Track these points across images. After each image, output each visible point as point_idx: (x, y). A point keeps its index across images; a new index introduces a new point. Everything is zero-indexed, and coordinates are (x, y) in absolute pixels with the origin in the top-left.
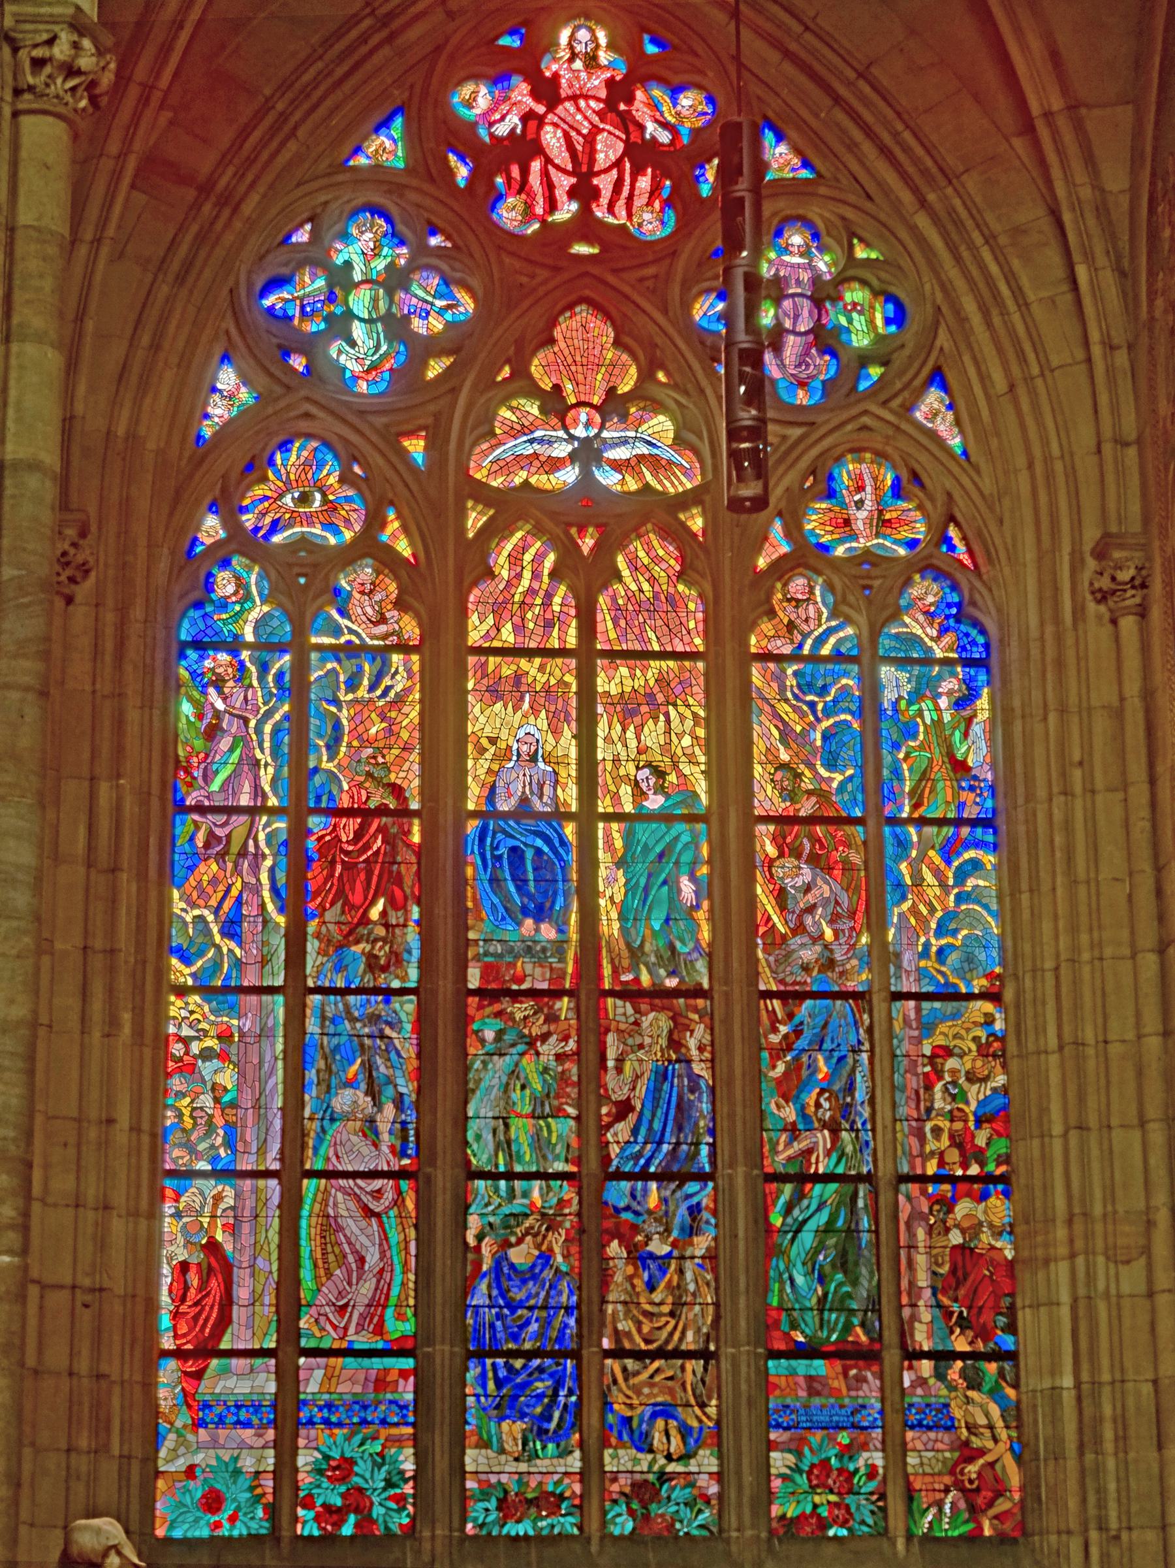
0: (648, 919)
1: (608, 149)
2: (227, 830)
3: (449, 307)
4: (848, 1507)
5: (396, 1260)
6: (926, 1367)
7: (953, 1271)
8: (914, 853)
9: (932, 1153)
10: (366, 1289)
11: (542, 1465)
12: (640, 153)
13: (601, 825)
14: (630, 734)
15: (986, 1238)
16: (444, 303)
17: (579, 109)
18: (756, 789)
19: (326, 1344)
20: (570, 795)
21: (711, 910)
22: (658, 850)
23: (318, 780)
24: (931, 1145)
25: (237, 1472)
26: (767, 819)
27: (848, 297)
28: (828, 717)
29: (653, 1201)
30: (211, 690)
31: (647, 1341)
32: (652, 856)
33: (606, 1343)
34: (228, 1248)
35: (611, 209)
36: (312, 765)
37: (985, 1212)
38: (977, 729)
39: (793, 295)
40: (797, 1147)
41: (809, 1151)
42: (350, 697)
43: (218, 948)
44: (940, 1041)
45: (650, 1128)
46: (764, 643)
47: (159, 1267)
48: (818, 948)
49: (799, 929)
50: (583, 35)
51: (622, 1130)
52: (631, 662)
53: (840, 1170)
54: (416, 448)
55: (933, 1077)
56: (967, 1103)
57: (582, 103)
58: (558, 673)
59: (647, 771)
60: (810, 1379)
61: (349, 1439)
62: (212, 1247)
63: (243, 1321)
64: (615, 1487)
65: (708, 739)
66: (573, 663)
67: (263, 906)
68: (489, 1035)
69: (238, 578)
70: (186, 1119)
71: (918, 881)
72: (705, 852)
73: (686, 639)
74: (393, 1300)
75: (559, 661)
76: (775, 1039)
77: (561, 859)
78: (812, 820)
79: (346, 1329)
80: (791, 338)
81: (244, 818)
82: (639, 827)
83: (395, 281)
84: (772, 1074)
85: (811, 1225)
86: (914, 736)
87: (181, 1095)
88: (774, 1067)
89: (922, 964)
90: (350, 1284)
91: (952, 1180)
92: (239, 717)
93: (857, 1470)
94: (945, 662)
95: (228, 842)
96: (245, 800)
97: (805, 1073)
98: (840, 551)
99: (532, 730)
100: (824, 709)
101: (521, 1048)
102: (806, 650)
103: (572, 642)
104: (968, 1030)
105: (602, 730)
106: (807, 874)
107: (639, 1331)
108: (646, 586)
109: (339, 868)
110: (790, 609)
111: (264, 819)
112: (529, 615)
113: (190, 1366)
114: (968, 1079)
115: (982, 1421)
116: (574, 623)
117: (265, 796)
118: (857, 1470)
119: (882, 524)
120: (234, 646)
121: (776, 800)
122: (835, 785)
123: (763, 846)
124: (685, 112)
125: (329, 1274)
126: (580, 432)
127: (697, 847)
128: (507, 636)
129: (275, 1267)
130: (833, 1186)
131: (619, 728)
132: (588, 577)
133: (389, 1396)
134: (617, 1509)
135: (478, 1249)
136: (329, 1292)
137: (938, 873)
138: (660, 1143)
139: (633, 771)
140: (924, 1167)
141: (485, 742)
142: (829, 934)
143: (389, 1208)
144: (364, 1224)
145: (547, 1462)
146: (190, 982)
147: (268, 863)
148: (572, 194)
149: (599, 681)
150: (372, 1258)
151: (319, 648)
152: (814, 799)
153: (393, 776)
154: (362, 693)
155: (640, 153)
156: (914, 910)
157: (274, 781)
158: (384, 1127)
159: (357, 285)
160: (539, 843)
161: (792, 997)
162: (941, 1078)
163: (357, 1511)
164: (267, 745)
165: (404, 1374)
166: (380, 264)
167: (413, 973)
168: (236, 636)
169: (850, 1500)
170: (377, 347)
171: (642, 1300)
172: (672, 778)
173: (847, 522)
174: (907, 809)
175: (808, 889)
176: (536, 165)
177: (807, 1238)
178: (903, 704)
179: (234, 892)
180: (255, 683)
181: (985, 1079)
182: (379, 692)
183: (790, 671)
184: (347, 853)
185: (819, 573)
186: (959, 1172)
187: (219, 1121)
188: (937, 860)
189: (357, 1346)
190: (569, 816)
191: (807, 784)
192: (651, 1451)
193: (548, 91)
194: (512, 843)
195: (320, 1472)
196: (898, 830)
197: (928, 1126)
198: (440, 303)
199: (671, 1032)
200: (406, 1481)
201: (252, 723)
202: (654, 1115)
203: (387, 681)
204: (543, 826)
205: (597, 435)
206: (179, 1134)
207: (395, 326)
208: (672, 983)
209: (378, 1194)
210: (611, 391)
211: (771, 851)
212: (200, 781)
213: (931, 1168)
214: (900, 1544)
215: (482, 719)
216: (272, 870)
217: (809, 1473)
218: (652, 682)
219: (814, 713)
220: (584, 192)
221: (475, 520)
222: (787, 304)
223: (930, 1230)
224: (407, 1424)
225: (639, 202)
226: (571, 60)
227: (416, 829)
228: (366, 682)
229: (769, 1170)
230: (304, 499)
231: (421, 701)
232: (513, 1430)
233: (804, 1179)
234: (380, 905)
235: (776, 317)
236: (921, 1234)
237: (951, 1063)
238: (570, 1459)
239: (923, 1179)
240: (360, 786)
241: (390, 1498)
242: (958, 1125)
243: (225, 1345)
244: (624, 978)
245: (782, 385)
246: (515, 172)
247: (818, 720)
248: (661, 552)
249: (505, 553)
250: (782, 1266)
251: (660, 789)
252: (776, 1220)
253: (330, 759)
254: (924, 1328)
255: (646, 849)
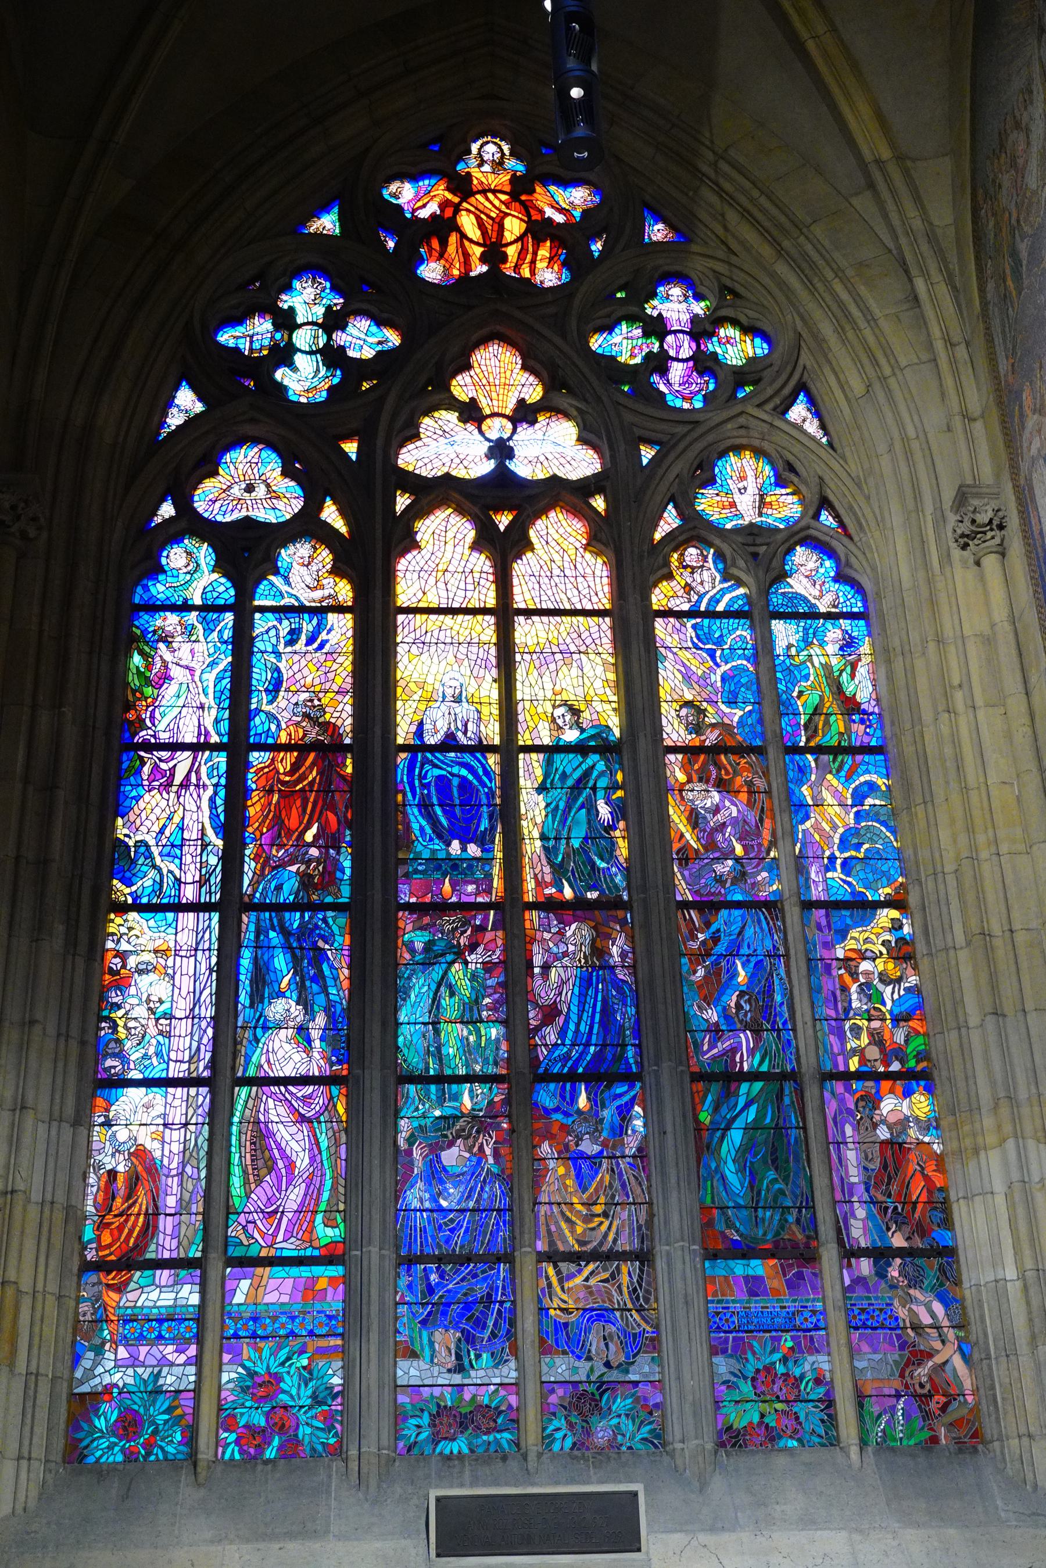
0: (568, 839)
1: (514, 227)
2: (171, 764)
3: (380, 343)
4: (797, 1418)
5: (325, 1163)
6: (865, 1266)
7: (885, 1166)
8: (813, 777)
9: (854, 1051)
10: (294, 1196)
11: (476, 1376)
12: (539, 230)
13: (521, 756)
14: (546, 678)
15: (913, 1133)
16: (375, 340)
17: (487, 199)
18: (664, 722)
19: (253, 1251)
20: (492, 733)
21: (627, 829)
22: (576, 775)
23: (257, 720)
24: (852, 1044)
25: (158, 1391)
26: (674, 750)
27: (722, 332)
28: (726, 663)
29: (582, 1101)
30: (161, 645)
31: (581, 1243)
32: (570, 782)
33: (541, 1246)
34: (157, 1154)
35: (517, 268)
36: (253, 706)
37: (910, 1107)
38: (862, 671)
39: (675, 332)
40: (721, 1046)
41: (735, 1049)
42: (289, 649)
43: (160, 870)
44: (851, 944)
45: (577, 1031)
46: (664, 602)
47: (85, 1177)
48: (730, 863)
49: (710, 845)
50: (491, 148)
51: (551, 1035)
52: (545, 619)
53: (764, 1068)
54: (351, 448)
55: (847, 979)
56: (884, 1003)
57: (490, 196)
58: (479, 629)
59: (561, 710)
60: (746, 1278)
61: (275, 1354)
62: (140, 1154)
63: (169, 1231)
64: (553, 1399)
65: (617, 681)
66: (491, 619)
67: (203, 829)
68: (419, 946)
69: (189, 554)
70: (120, 1029)
71: (819, 804)
72: (619, 777)
73: (595, 599)
74: (323, 1207)
75: (480, 617)
76: (694, 945)
77: (484, 785)
78: (717, 749)
79: (275, 1235)
80: (675, 364)
81: (187, 754)
82: (558, 758)
83: (333, 322)
84: (693, 978)
85: (739, 1123)
86: (806, 677)
87: (119, 1007)
88: (695, 972)
89: (829, 875)
90: (279, 1190)
91: (877, 1077)
92: (187, 667)
93: (802, 1376)
94: (828, 616)
95: (173, 775)
96: (190, 738)
97: (724, 978)
98: (729, 526)
99: (457, 676)
100: (722, 655)
101: (449, 958)
102: (702, 609)
103: (491, 602)
104: (878, 935)
105: (520, 674)
106: (716, 797)
107: (573, 1232)
108: (556, 557)
109: (276, 797)
110: (686, 573)
111: (207, 753)
112: (452, 581)
113: (112, 1279)
114: (881, 981)
115: (927, 1320)
116: (493, 587)
117: (207, 734)
118: (802, 1376)
119: (762, 503)
120: (185, 607)
121: (682, 732)
122: (736, 719)
123: (673, 772)
124: (577, 202)
125: (259, 1182)
126: (494, 435)
127: (612, 774)
128: (432, 600)
129: (203, 1174)
130: (758, 1085)
131: (536, 673)
132: (504, 549)
133: (318, 1306)
134: (556, 1423)
135: (409, 1152)
136: (259, 1197)
137: (836, 794)
138: (588, 1045)
139: (550, 710)
140: (847, 1065)
141: (412, 685)
142: (739, 850)
143: (319, 1114)
144: (294, 1129)
145: (481, 1373)
146: (130, 901)
147: (210, 791)
148: (483, 259)
149: (517, 634)
150: (302, 1162)
151: (263, 610)
152: (717, 732)
153: (328, 716)
154: (300, 646)
155: (539, 230)
156: (817, 827)
157: (217, 721)
158: (315, 1034)
159: (300, 326)
160: (464, 772)
161: (708, 906)
162: (856, 980)
163: (282, 1429)
164: (211, 691)
165: (332, 1280)
166: (319, 311)
167: (346, 891)
168: (186, 600)
169: (798, 1408)
170: (318, 370)
171: (575, 1200)
172: (586, 715)
173: (733, 505)
174: (804, 739)
175: (716, 810)
176: (453, 239)
177: (736, 1136)
178: (793, 651)
179: (177, 819)
180: (202, 638)
181: (899, 980)
182: (315, 645)
183: (689, 625)
184: (283, 783)
185: (710, 545)
186: (882, 1069)
187: (152, 1030)
188: (835, 782)
189: (286, 1253)
190: (493, 749)
191: (710, 719)
192: (589, 1359)
193: (463, 187)
194: (437, 772)
195: (244, 1390)
196: (797, 757)
197: (847, 1025)
198: (370, 340)
199: (593, 941)
200: (335, 1396)
201: (197, 674)
202: (580, 1018)
203: (323, 636)
204: (467, 758)
205: (510, 438)
206: (112, 1045)
207: (332, 356)
208: (592, 895)
209: (306, 1100)
210: (521, 402)
211: (682, 777)
212: (148, 722)
213: (854, 1064)
214: (854, 1451)
215: (411, 667)
216: (212, 800)
217: (753, 1379)
218: (564, 634)
219: (713, 656)
220: (494, 252)
221: (402, 502)
222: (670, 339)
223: (857, 1127)
224: (336, 1335)
225: (541, 265)
226: (480, 166)
227: (349, 761)
228: (303, 639)
229: (696, 1069)
230: (250, 489)
231: (354, 652)
232: (445, 1339)
233: (729, 1078)
234: (314, 830)
235: (661, 346)
236: (849, 1130)
237: (865, 966)
238: (505, 1370)
239: (847, 1076)
240: (297, 724)
241: (315, 1417)
242: (876, 1024)
243: (150, 1256)
244: (547, 891)
245: (669, 397)
246: (435, 244)
247: (718, 666)
248: (569, 529)
249: (430, 531)
250: (713, 1165)
251: (578, 725)
252: (704, 1117)
253: (271, 702)
254: (860, 1224)
255: (564, 776)
